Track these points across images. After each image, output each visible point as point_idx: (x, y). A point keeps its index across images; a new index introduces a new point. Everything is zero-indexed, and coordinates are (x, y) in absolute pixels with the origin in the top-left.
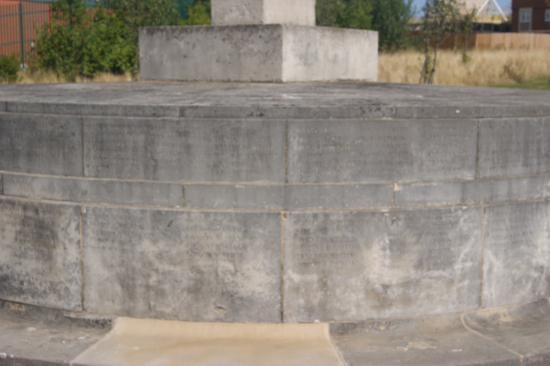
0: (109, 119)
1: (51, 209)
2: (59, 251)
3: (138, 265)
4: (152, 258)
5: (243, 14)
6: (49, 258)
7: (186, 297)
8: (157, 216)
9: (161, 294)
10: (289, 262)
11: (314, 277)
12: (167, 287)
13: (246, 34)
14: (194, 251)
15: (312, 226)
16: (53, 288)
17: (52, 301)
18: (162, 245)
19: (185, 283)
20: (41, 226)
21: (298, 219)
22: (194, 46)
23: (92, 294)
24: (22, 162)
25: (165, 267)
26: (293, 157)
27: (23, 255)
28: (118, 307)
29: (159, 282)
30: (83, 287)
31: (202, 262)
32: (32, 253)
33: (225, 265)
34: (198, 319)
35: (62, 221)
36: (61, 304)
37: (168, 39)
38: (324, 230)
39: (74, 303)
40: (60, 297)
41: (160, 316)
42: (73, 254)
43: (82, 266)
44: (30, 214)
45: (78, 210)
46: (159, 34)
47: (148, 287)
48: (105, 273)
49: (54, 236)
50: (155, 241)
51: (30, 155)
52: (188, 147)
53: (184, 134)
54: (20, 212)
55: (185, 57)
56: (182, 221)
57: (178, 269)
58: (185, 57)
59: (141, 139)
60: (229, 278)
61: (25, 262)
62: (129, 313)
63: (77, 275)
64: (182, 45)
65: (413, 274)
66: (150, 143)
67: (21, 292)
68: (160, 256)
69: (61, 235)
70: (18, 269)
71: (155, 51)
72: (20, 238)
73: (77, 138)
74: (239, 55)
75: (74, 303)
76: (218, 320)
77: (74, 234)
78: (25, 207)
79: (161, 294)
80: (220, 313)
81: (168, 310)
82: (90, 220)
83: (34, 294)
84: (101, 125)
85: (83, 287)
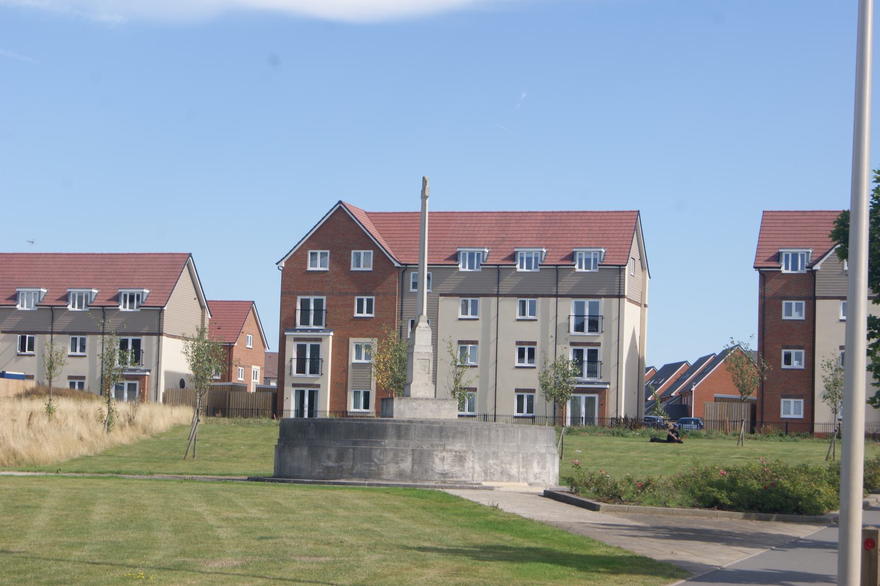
0: (479, 427)
1: (465, 452)
2: (467, 464)
3: (488, 466)
4: (492, 464)
5: (426, 393)
6: (463, 466)
7: (500, 475)
8: (494, 453)
9: (494, 474)
10: (521, 466)
11: (525, 470)
12: (495, 472)
13: (443, 402)
14: (502, 462)
15: (525, 456)
16: (464, 475)
17: (463, 479)
18: (494, 461)
19: (500, 471)
20: (461, 457)
21: (523, 454)
22: (420, 405)
23: (476, 476)
24: (451, 439)
25: (495, 467)
26: (519, 438)
27: (455, 466)
28: (483, 479)
29: (494, 471)
30: (473, 474)
31: (503, 466)
32: (458, 465)
33: (508, 466)
34: (502, 481)
35: (468, 455)
36: (466, 479)
37: (408, 402)
38: (527, 457)
39: (470, 479)
40: (466, 477)
41: (493, 481)
42: (471, 464)
43: (473, 468)
44: (457, 454)
45: (473, 452)
46: (404, 400)
47: (491, 473)
48: (480, 469)
49: (465, 459)
50: (493, 460)
51: (453, 437)
52: (498, 435)
53: (497, 431)
54: (454, 453)
55: (416, 409)
56: (500, 454)
57: (498, 468)
58: (416, 409)
59: (487, 432)
60: (509, 470)
61: (454, 468)
62: (485, 480)
63: (472, 471)
64: (414, 404)
65: (541, 471)
66: (489, 434)
67: (452, 477)
68: (494, 464)
69: (467, 459)
70: (452, 470)
71: (402, 406)
72: (453, 461)
73: (470, 432)
74: (440, 410)
75: (470, 479)
76: (506, 482)
77: (471, 459)
78: (456, 452)
79: (494, 474)
80: (507, 480)
81: (495, 479)
82: (476, 454)
83: (457, 477)
84: (477, 429)
85: (473, 474)
